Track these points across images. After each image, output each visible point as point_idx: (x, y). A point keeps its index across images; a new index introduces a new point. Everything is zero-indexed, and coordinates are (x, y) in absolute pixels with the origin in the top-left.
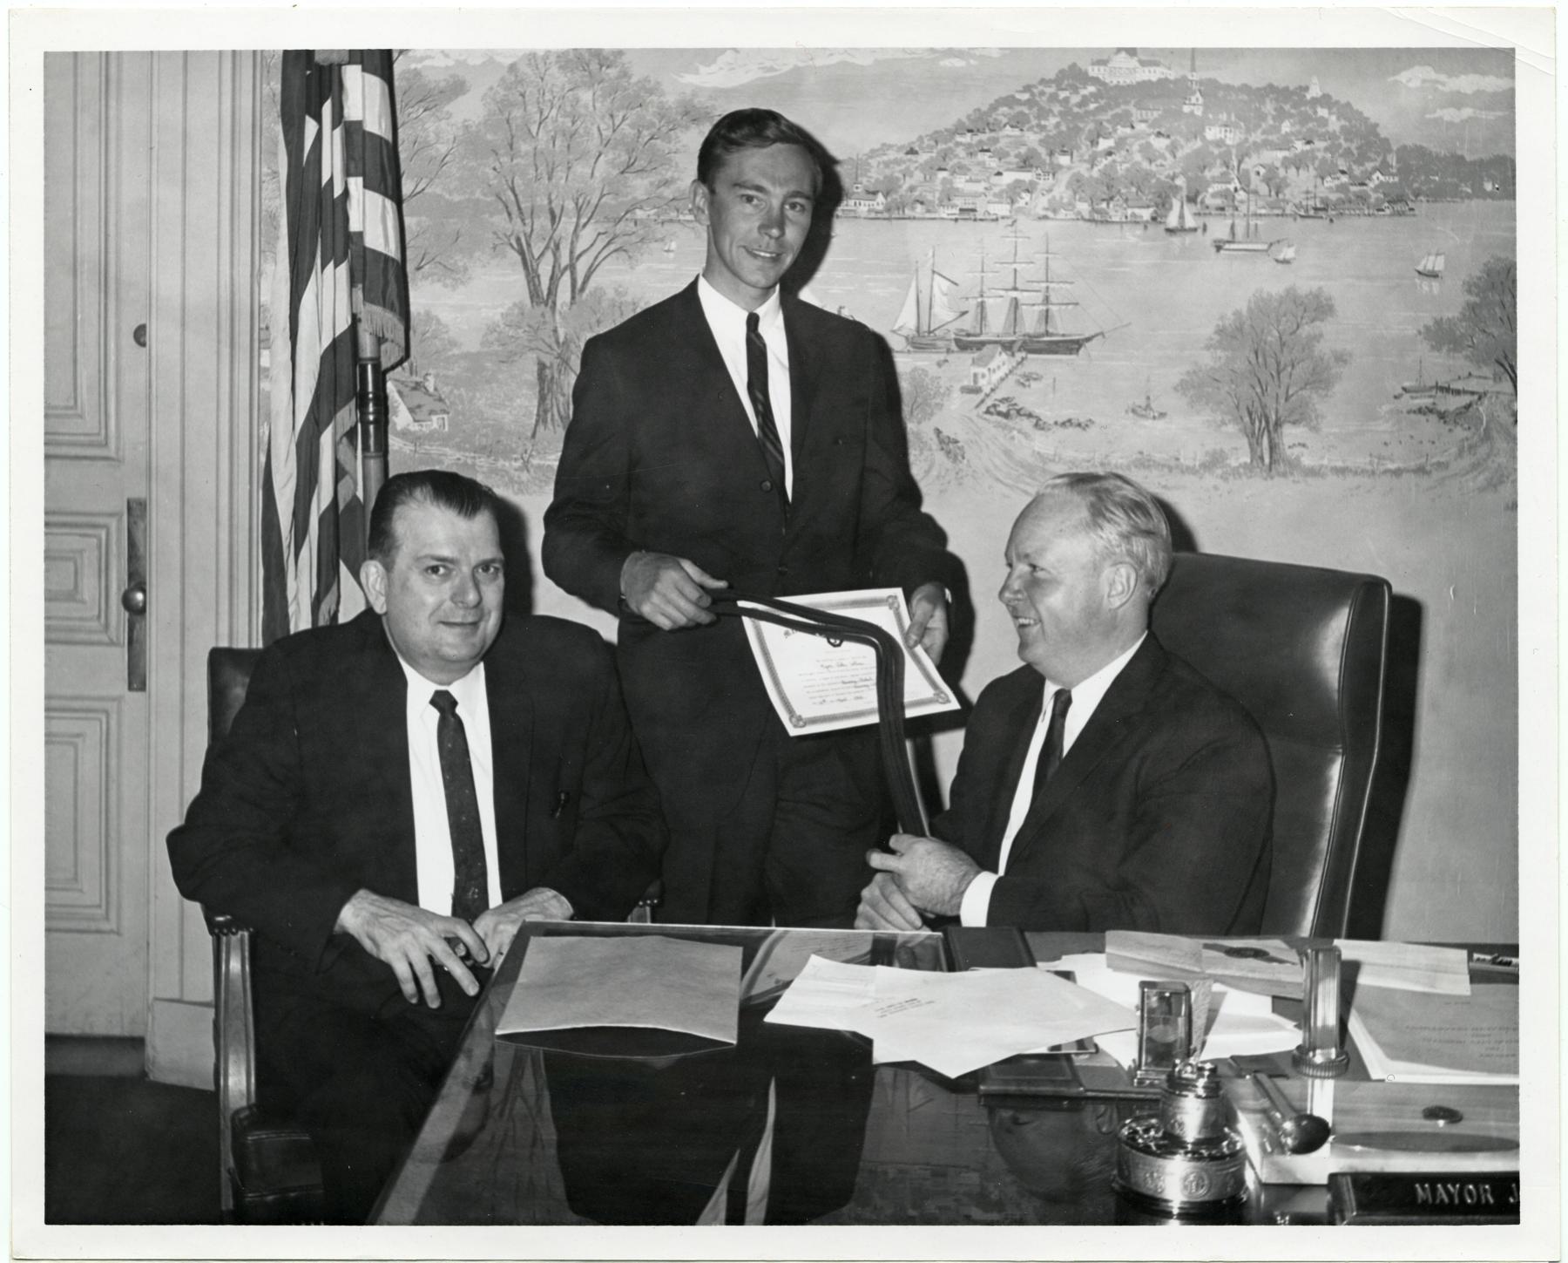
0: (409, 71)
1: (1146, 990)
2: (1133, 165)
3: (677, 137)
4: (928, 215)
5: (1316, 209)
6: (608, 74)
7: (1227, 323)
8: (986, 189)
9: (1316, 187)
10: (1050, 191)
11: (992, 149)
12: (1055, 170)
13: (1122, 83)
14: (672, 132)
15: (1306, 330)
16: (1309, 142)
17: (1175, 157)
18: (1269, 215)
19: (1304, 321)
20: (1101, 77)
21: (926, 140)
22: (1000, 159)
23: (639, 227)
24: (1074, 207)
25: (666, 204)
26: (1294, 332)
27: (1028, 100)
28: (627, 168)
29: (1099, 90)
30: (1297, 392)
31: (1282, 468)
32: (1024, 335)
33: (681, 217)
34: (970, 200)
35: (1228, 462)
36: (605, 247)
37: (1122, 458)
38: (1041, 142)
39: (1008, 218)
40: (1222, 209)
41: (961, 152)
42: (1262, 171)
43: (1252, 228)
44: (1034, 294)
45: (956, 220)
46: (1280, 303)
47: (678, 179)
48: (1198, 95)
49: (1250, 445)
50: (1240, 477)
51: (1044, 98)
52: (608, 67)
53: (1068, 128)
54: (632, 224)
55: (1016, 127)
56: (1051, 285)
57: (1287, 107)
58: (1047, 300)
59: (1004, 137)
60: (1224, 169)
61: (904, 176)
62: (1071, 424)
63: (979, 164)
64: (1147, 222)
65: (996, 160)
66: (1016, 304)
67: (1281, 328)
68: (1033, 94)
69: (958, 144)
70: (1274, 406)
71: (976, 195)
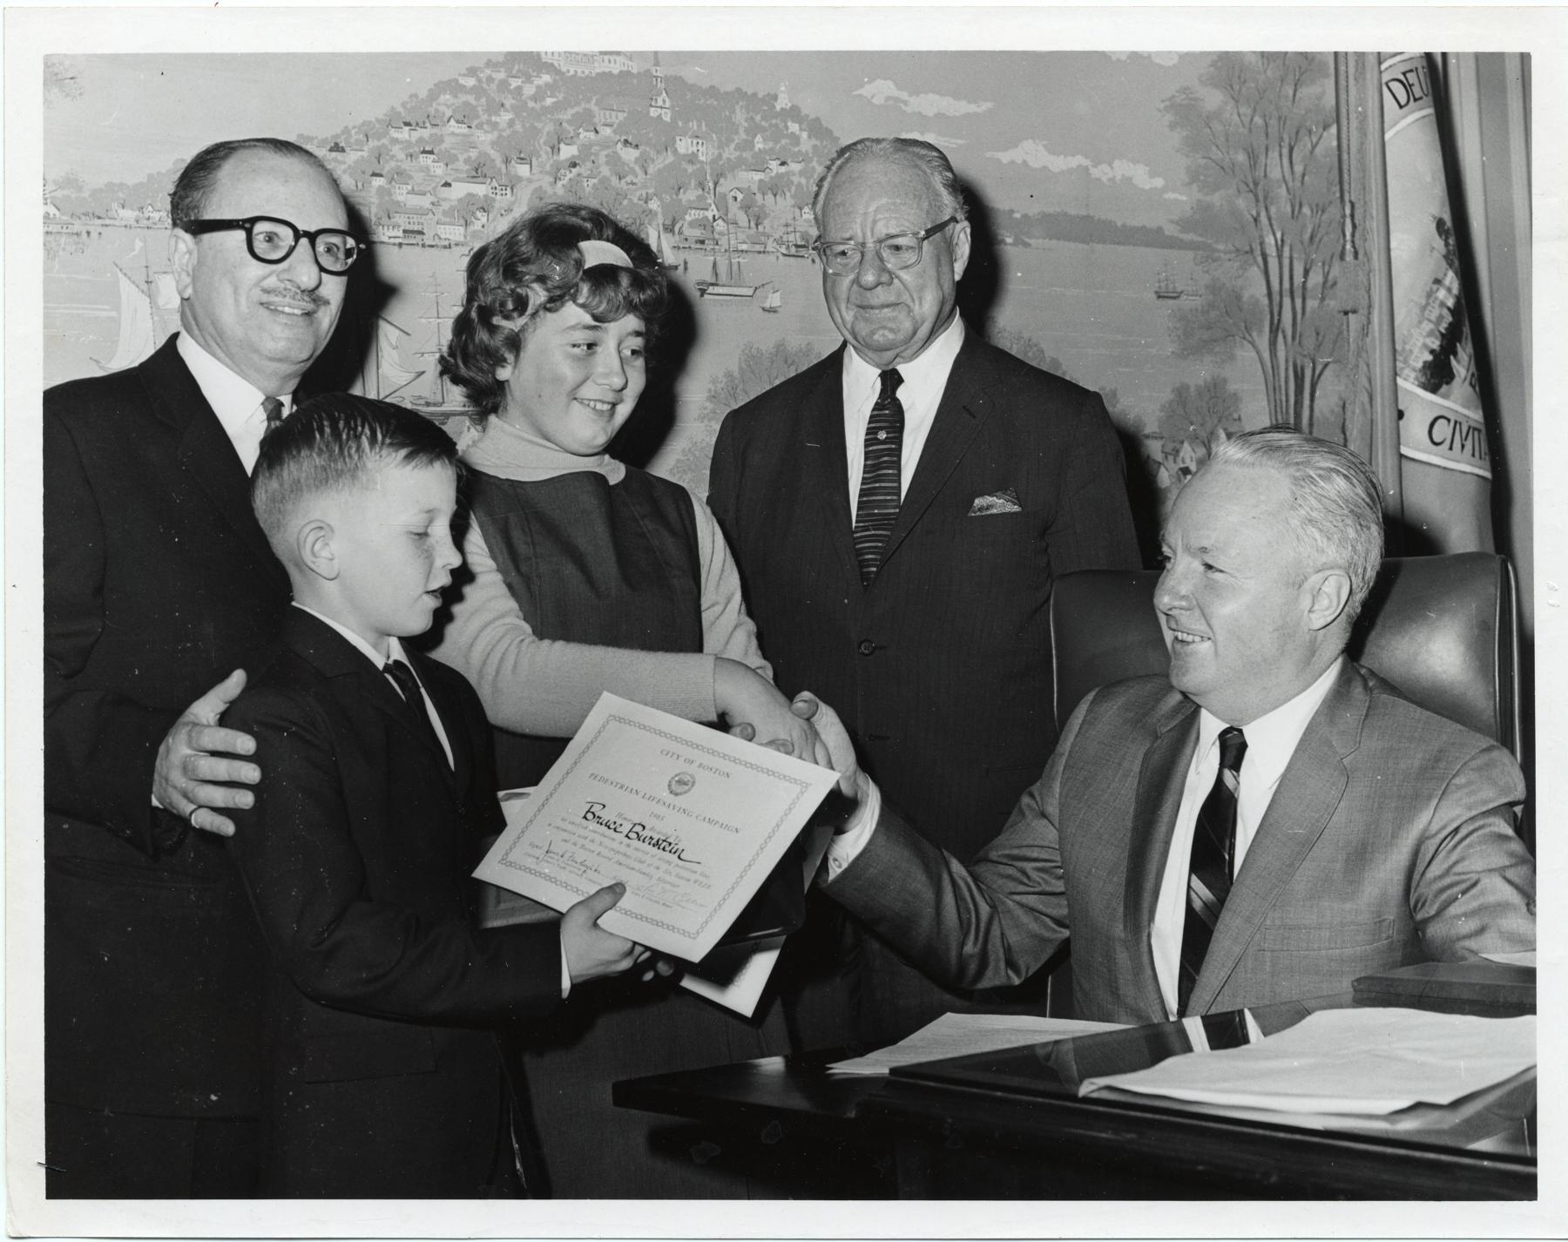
5: (797, 246)
7: (720, 386)
8: (433, 204)
10: (509, 210)
11: (435, 151)
12: (512, 184)
13: (579, 71)
16: (783, 164)
17: (646, 174)
20: (556, 64)
21: (353, 132)
27: (474, 86)
29: (555, 81)
34: (416, 219)
38: (493, 144)
40: (702, 242)
42: (740, 196)
43: (735, 268)
45: (400, 245)
46: (772, 362)
48: (664, 94)
53: (523, 126)
55: (462, 122)
57: (758, 118)
60: (700, 192)
65: (442, 164)
68: (479, 80)
71: (422, 212)
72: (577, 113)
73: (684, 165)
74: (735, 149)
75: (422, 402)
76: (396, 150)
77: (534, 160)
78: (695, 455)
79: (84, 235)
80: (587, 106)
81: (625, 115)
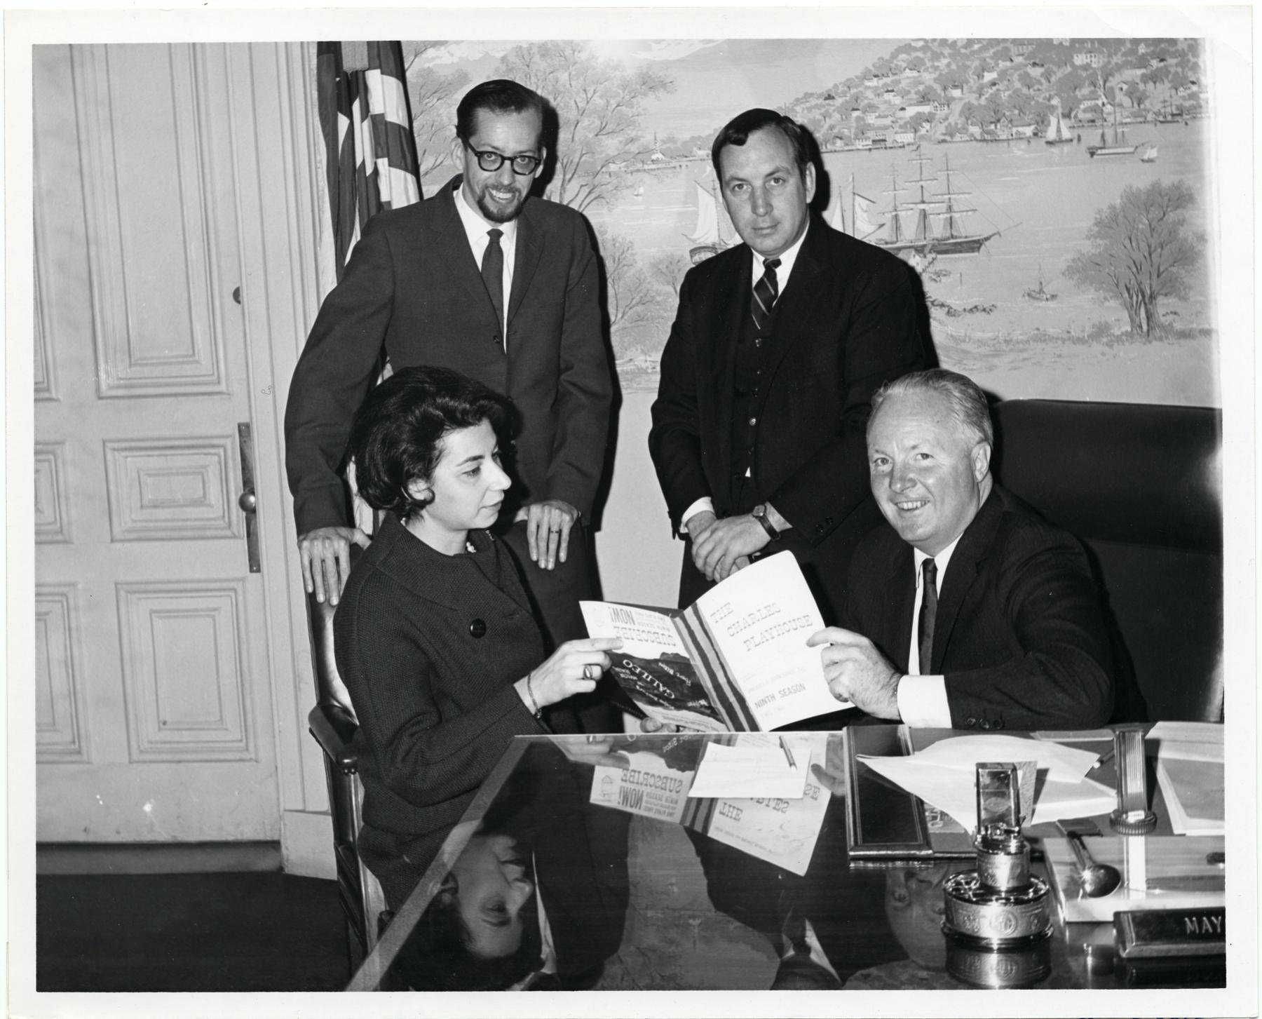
0: (424, 70)
1: (980, 770)
2: (1014, 92)
3: (638, 103)
4: (846, 148)
5: (1173, 115)
6: (579, 57)
7: (1104, 216)
8: (893, 122)
9: (1171, 96)
10: (946, 119)
12: (949, 102)
14: (633, 100)
15: (1172, 216)
16: (1162, 60)
17: (1049, 82)
18: (1133, 123)
19: (1169, 209)
21: (840, 87)
22: (903, 97)
23: (613, 178)
24: (967, 130)
25: (633, 158)
26: (1162, 219)
28: (600, 131)
30: (1167, 269)
31: (1158, 333)
32: (933, 240)
33: (646, 167)
34: (881, 132)
35: (1112, 331)
36: (585, 198)
37: (1021, 335)
38: (936, 80)
39: (912, 144)
40: (1093, 121)
41: (869, 94)
42: (1125, 87)
44: (937, 205)
45: (870, 150)
47: (642, 136)
49: (1130, 316)
50: (1123, 344)
51: (936, 44)
52: (579, 52)
53: (957, 66)
54: (608, 176)
56: (952, 196)
58: (950, 209)
59: (904, 78)
60: (1093, 88)
61: (825, 118)
62: (978, 310)
63: (885, 102)
64: (1030, 137)
65: (899, 97)
66: (924, 215)
67: (1150, 216)
69: (867, 88)
70: (1148, 282)
71: (885, 128)
72: (998, 51)
73: (1080, 72)
74: (1123, 56)
75: (883, 242)
76: (869, 94)
77: (965, 87)
78: (1082, 262)
79: (678, 167)
80: (1005, 45)
81: (1034, 46)
